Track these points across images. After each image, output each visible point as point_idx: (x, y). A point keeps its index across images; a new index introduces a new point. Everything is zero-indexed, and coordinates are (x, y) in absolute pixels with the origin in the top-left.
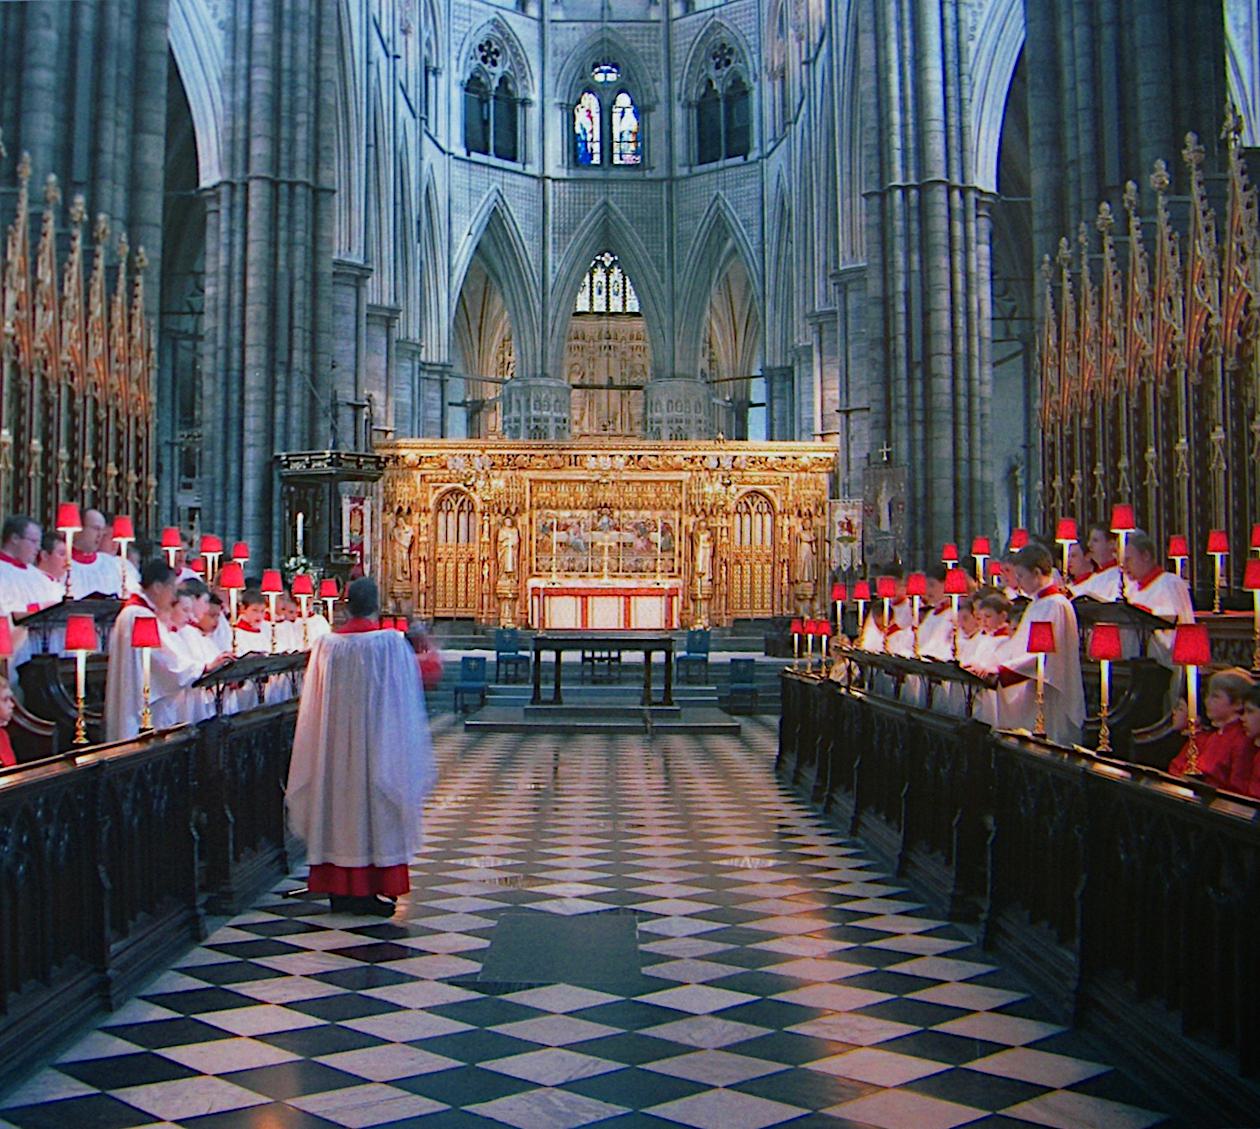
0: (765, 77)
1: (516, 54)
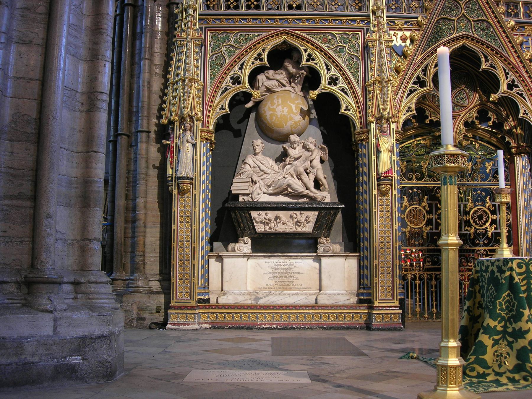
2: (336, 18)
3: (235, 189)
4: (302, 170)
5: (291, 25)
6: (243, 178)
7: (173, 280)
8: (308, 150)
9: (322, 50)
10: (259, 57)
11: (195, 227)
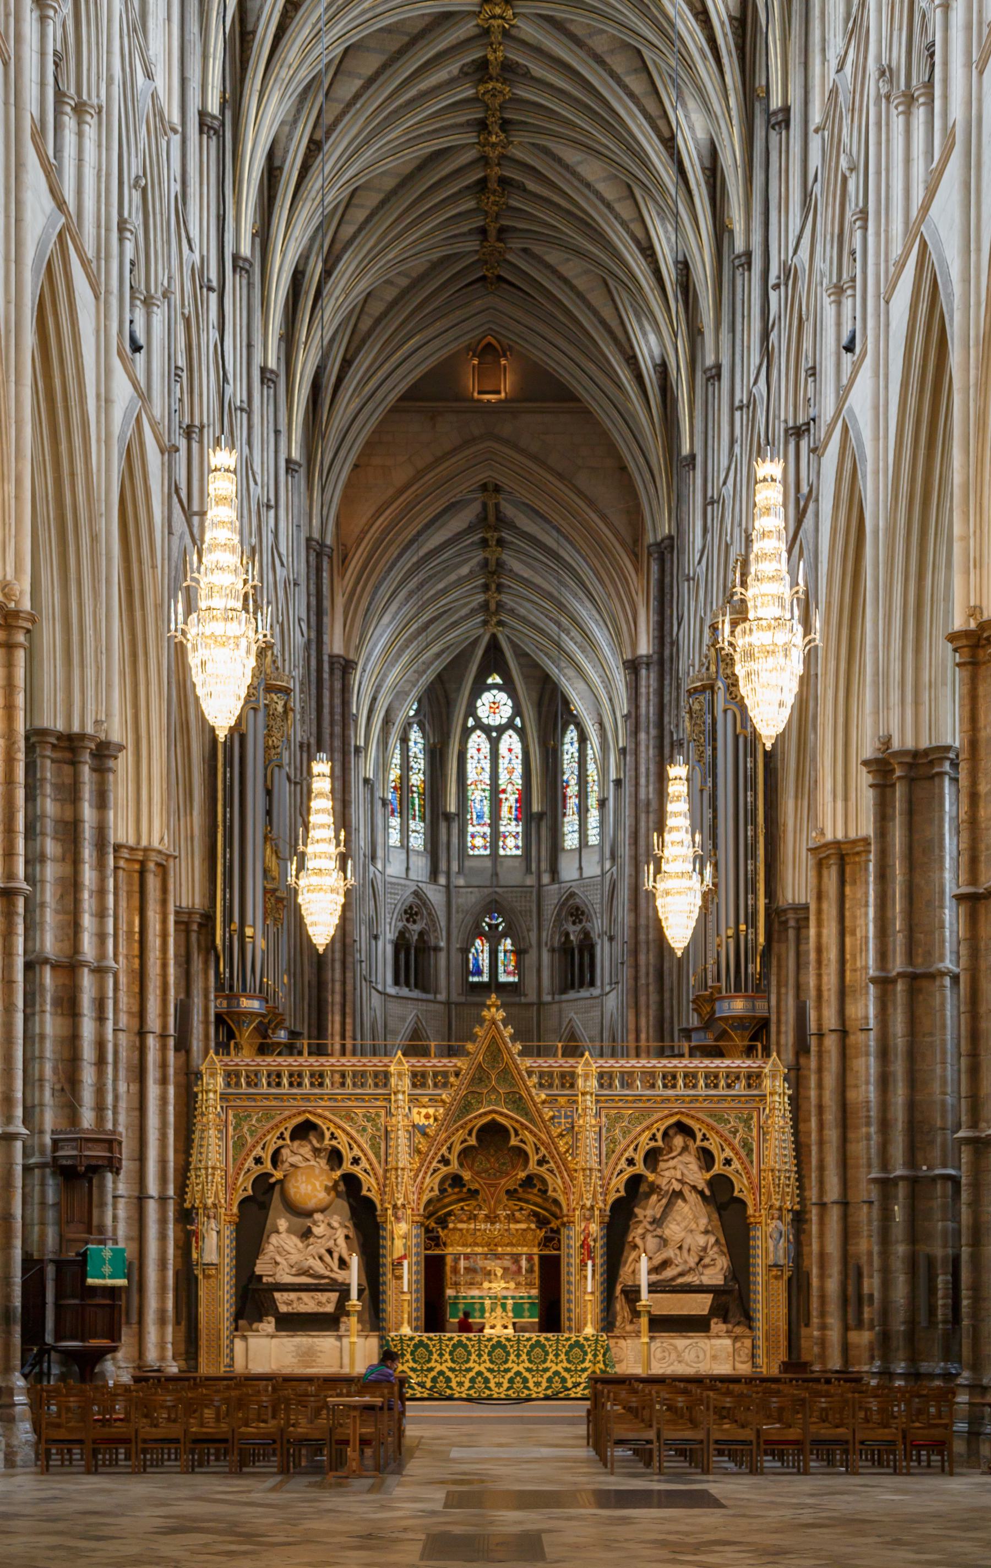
0: (606, 939)
1: (430, 914)
2: (359, 1098)
3: (258, 1270)
4: (323, 1251)
5: (313, 1104)
6: (267, 1257)
7: (201, 1360)
8: (333, 1228)
9: (344, 1130)
10: (281, 1137)
11: (220, 1310)
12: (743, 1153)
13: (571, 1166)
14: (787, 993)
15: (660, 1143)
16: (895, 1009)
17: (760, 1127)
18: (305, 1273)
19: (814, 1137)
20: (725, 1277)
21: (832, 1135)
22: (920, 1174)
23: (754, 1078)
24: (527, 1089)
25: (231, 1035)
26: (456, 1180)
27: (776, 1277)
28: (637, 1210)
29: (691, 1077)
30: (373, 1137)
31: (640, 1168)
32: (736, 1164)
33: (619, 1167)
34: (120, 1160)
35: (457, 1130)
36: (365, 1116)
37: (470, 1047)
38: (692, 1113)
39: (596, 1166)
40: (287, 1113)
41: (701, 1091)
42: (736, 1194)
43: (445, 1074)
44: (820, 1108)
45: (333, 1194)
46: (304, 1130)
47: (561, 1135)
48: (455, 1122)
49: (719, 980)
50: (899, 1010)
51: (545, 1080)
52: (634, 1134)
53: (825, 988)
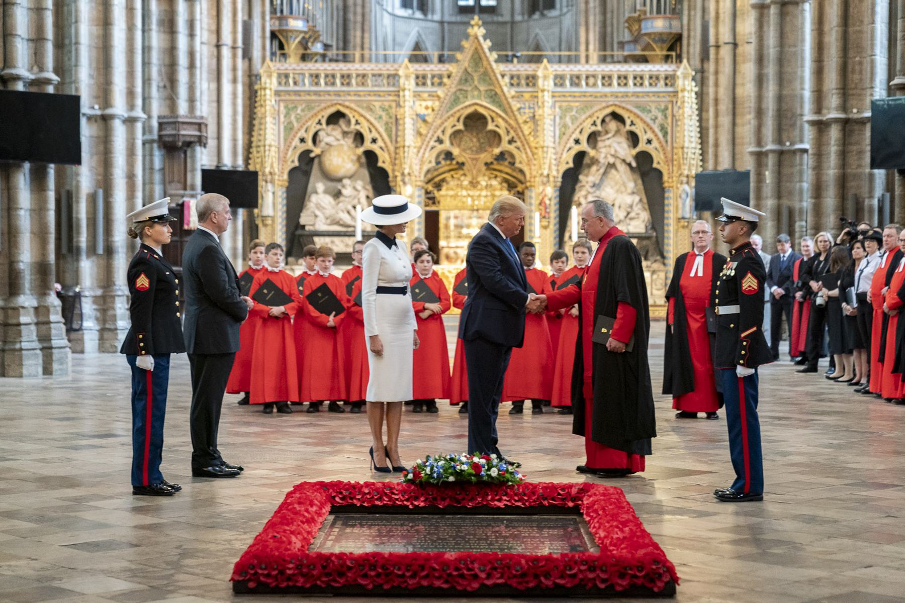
2: (377, 94)
4: (350, 207)
5: (343, 98)
10: (319, 123)
12: (660, 135)
13: (533, 145)
14: (695, 15)
15: (599, 128)
16: (769, 27)
17: (673, 116)
18: (338, 223)
19: (711, 122)
20: (646, 227)
21: (725, 120)
22: (785, 148)
23: (670, 79)
24: (501, 87)
25: (281, 47)
26: (449, 155)
27: (684, 227)
28: (581, 177)
29: (623, 78)
30: (387, 124)
31: (584, 146)
32: (655, 143)
33: (568, 146)
34: (206, 138)
35: (449, 118)
36: (381, 107)
37: (459, 56)
38: (624, 105)
39: (552, 145)
40: (323, 105)
41: (631, 88)
42: (655, 165)
43: (441, 77)
44: (716, 100)
45: (357, 165)
46: (336, 118)
47: (526, 122)
48: (447, 112)
49: (645, 5)
50: (772, 28)
51: (515, 80)
52: (580, 121)
53: (721, 11)
